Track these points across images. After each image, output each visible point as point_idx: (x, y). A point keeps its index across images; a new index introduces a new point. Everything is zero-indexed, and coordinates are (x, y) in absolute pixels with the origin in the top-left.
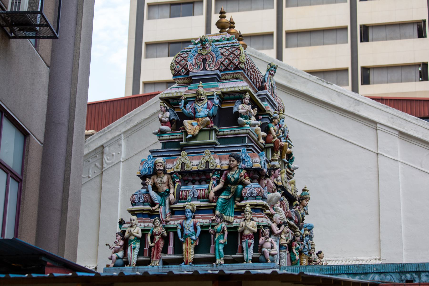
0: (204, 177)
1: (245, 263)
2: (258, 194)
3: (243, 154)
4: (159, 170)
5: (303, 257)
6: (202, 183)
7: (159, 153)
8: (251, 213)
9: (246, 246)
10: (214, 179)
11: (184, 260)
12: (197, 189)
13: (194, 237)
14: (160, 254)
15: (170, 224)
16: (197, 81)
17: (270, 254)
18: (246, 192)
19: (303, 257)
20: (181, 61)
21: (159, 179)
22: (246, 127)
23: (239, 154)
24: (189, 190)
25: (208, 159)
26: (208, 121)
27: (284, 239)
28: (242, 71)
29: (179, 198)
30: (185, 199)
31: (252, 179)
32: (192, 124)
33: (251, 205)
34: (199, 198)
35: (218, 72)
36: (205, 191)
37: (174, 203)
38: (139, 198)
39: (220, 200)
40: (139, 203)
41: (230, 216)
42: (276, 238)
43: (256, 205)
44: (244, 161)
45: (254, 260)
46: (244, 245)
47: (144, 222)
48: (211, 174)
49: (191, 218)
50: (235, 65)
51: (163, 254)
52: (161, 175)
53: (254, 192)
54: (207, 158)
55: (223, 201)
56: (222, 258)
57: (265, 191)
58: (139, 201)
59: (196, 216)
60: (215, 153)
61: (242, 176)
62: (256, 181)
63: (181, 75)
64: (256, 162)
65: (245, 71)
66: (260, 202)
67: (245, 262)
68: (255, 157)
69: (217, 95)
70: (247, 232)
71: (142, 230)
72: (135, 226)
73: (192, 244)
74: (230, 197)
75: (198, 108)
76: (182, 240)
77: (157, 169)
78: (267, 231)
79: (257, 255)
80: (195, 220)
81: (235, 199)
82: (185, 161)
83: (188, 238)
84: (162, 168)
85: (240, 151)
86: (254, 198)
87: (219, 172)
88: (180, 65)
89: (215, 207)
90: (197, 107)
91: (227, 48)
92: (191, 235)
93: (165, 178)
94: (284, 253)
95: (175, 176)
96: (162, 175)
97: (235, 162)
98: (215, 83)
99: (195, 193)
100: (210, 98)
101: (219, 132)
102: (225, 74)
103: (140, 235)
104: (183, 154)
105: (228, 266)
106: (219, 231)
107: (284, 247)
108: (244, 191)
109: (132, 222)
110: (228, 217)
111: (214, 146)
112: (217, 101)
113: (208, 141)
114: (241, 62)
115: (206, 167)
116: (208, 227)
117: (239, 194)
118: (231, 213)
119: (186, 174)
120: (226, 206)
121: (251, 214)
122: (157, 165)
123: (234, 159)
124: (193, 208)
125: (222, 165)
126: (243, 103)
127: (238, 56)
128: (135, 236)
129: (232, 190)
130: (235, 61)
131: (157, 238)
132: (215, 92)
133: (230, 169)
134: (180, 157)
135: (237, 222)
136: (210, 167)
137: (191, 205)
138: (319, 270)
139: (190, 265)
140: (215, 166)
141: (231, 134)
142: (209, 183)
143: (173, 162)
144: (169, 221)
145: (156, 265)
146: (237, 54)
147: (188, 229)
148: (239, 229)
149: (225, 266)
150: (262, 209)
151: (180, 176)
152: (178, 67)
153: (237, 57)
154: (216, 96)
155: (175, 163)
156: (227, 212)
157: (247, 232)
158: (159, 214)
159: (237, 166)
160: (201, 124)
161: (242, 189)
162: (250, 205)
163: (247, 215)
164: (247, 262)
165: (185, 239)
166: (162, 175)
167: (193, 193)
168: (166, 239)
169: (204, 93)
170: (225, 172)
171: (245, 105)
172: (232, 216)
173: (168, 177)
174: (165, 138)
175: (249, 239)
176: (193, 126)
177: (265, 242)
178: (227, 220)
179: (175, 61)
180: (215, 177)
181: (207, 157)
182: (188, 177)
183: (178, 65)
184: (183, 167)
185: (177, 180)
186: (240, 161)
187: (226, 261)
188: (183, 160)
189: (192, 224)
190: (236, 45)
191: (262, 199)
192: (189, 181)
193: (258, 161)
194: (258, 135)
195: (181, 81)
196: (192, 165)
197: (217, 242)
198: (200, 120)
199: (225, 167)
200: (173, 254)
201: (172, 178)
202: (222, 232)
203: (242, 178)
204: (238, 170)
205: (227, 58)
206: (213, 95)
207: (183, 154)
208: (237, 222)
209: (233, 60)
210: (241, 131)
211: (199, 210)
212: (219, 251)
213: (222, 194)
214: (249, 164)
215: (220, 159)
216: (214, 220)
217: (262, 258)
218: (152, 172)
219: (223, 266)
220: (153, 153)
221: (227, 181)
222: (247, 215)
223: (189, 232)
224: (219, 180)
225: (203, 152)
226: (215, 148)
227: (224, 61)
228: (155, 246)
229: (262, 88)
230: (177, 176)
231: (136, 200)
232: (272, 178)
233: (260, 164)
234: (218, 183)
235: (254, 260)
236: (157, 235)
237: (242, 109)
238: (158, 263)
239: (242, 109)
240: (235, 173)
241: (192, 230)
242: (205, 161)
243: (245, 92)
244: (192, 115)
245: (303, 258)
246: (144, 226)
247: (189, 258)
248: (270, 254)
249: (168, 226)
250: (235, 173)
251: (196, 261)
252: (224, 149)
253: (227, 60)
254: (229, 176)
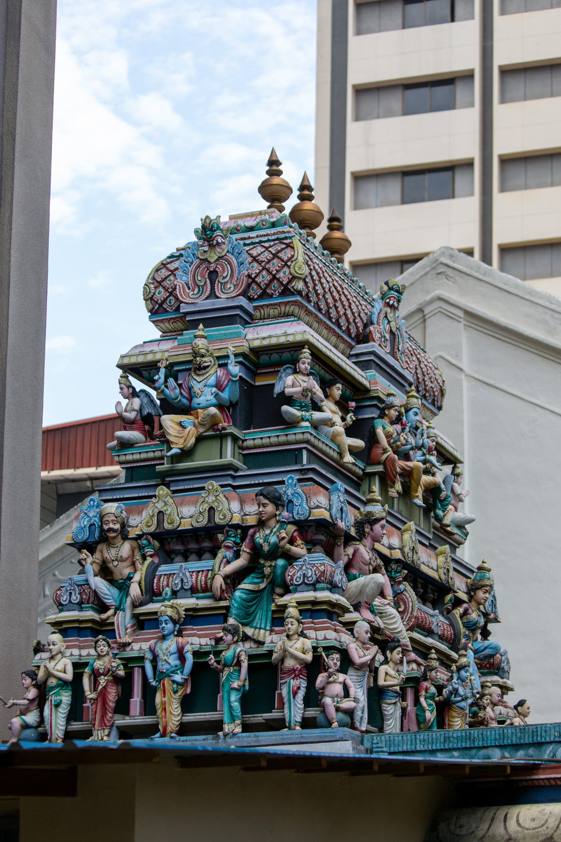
0: (207, 544)
1: (286, 729)
2: (320, 577)
3: (291, 488)
4: (110, 530)
5: (454, 714)
6: (204, 557)
7: (117, 492)
9: (289, 692)
10: (228, 547)
11: (160, 727)
12: (188, 571)
13: (178, 678)
14: (110, 715)
15: (132, 649)
16: (194, 325)
17: (338, 709)
18: (294, 574)
19: (454, 714)
20: (166, 278)
21: (113, 552)
22: (301, 427)
23: (281, 489)
24: (174, 574)
25: (213, 502)
26: (213, 416)
27: (391, 676)
28: (298, 298)
29: (151, 593)
30: (160, 594)
31: (311, 545)
32: (180, 424)
33: (299, 603)
34: (194, 591)
35: (243, 301)
36: (207, 575)
37: (141, 604)
38: (71, 593)
39: (238, 594)
40: (70, 606)
41: (260, 628)
42: (360, 673)
43: (314, 603)
44: (291, 504)
45: (307, 723)
46: (284, 691)
47: (80, 648)
48: (220, 537)
49: (172, 636)
50: (281, 283)
51: (117, 716)
52: (116, 541)
53: (309, 575)
54: (210, 501)
55: (244, 596)
56: (238, 722)
57: (338, 571)
58: (70, 602)
59: (185, 630)
60: (235, 488)
61: (283, 538)
62: (318, 548)
63: (166, 311)
64: (318, 507)
66: (324, 595)
67: (286, 727)
68: (315, 494)
69: (236, 355)
70: (290, 663)
71: (75, 665)
72: (60, 655)
73: (175, 692)
74: (262, 586)
75: (197, 388)
76: (154, 683)
77: (106, 527)
78: (333, 661)
79: (312, 712)
80: (180, 639)
81: (273, 592)
82: (165, 508)
83: (166, 679)
84: (117, 526)
85: (282, 482)
86: (311, 587)
87: (239, 531)
88: (164, 288)
89: (228, 608)
90: (193, 383)
91: (267, 245)
92: (173, 672)
93: (126, 549)
94: (391, 706)
95: (145, 542)
96: (119, 541)
97: (270, 508)
98: (238, 328)
99: (185, 581)
100: (222, 362)
101: (243, 441)
102: (262, 306)
103: (69, 676)
104: (161, 492)
105: (250, 737)
106: (229, 663)
107: (391, 694)
108: (291, 572)
109: (51, 647)
110: (257, 630)
111: (231, 472)
112: (235, 369)
113: (217, 461)
114: (294, 278)
115: (209, 521)
116: (207, 653)
117: (279, 580)
118: (263, 622)
119: (172, 538)
120: (254, 607)
121: (299, 622)
122: (105, 519)
123: (267, 501)
124: (178, 613)
125: (245, 515)
126: (297, 373)
127: (289, 263)
128: (59, 679)
129: (267, 571)
130: (281, 275)
131: (103, 681)
132: (231, 348)
133: (261, 524)
134: (154, 500)
135: (273, 641)
136: (217, 520)
137: (172, 607)
138: (442, 740)
139: (172, 737)
140: (228, 518)
142: (214, 556)
143: (140, 513)
144: (129, 644)
145: (102, 739)
146: (285, 259)
147: (165, 660)
148: (275, 656)
149: (243, 737)
150: (332, 611)
151: (157, 544)
152: (159, 293)
153: (286, 264)
154: (232, 357)
155: (144, 513)
156: (256, 621)
157: (290, 663)
158: (114, 630)
159: (276, 515)
160: (201, 424)
161: (285, 569)
162: (297, 602)
163: (290, 626)
164: (289, 728)
165: (160, 680)
166: (119, 541)
167: (182, 580)
168: (124, 684)
169: (208, 351)
170: (251, 531)
171: (300, 377)
172: (265, 629)
173: (131, 545)
174: (129, 458)
175: (293, 678)
176: (184, 428)
177: (329, 683)
178: (255, 637)
179: (154, 278)
180: (229, 543)
181: (211, 498)
182: (172, 543)
183: (161, 289)
184: (160, 522)
185: (149, 551)
186: (283, 506)
187: (247, 728)
188: (160, 505)
189: (173, 648)
190: (286, 238)
191: (330, 591)
192: (177, 553)
193: (325, 503)
195: (167, 325)
196: (182, 518)
197: (227, 686)
198: (199, 414)
199: (252, 521)
200: (141, 715)
201: (141, 548)
202: (235, 665)
203: (282, 543)
204: (278, 526)
205: (264, 268)
206: (227, 357)
207: (161, 492)
208: (272, 642)
209: (278, 271)
210: (291, 438)
211: (193, 617)
212: (230, 707)
213: (245, 581)
214: (301, 510)
215: (242, 502)
216: (221, 639)
217: (321, 719)
218: (97, 535)
219: (239, 737)
220: (103, 494)
221: (256, 552)
222: (290, 626)
223: (167, 666)
224: (239, 550)
225: (203, 488)
226: (234, 478)
227: (257, 275)
228: (97, 698)
230: (150, 542)
231: (64, 599)
233: (329, 510)
234: (237, 555)
235: (307, 723)
236: (102, 674)
237: (293, 386)
238: (108, 735)
239: (293, 386)
240: (271, 531)
241: (174, 661)
242: (206, 506)
243: (299, 346)
244: (184, 405)
245: (454, 717)
246: (80, 656)
247: (170, 724)
248: (338, 709)
249: (129, 653)
250: (271, 531)
251: (185, 729)
252: (254, 478)
253: (264, 273)
254: (258, 540)
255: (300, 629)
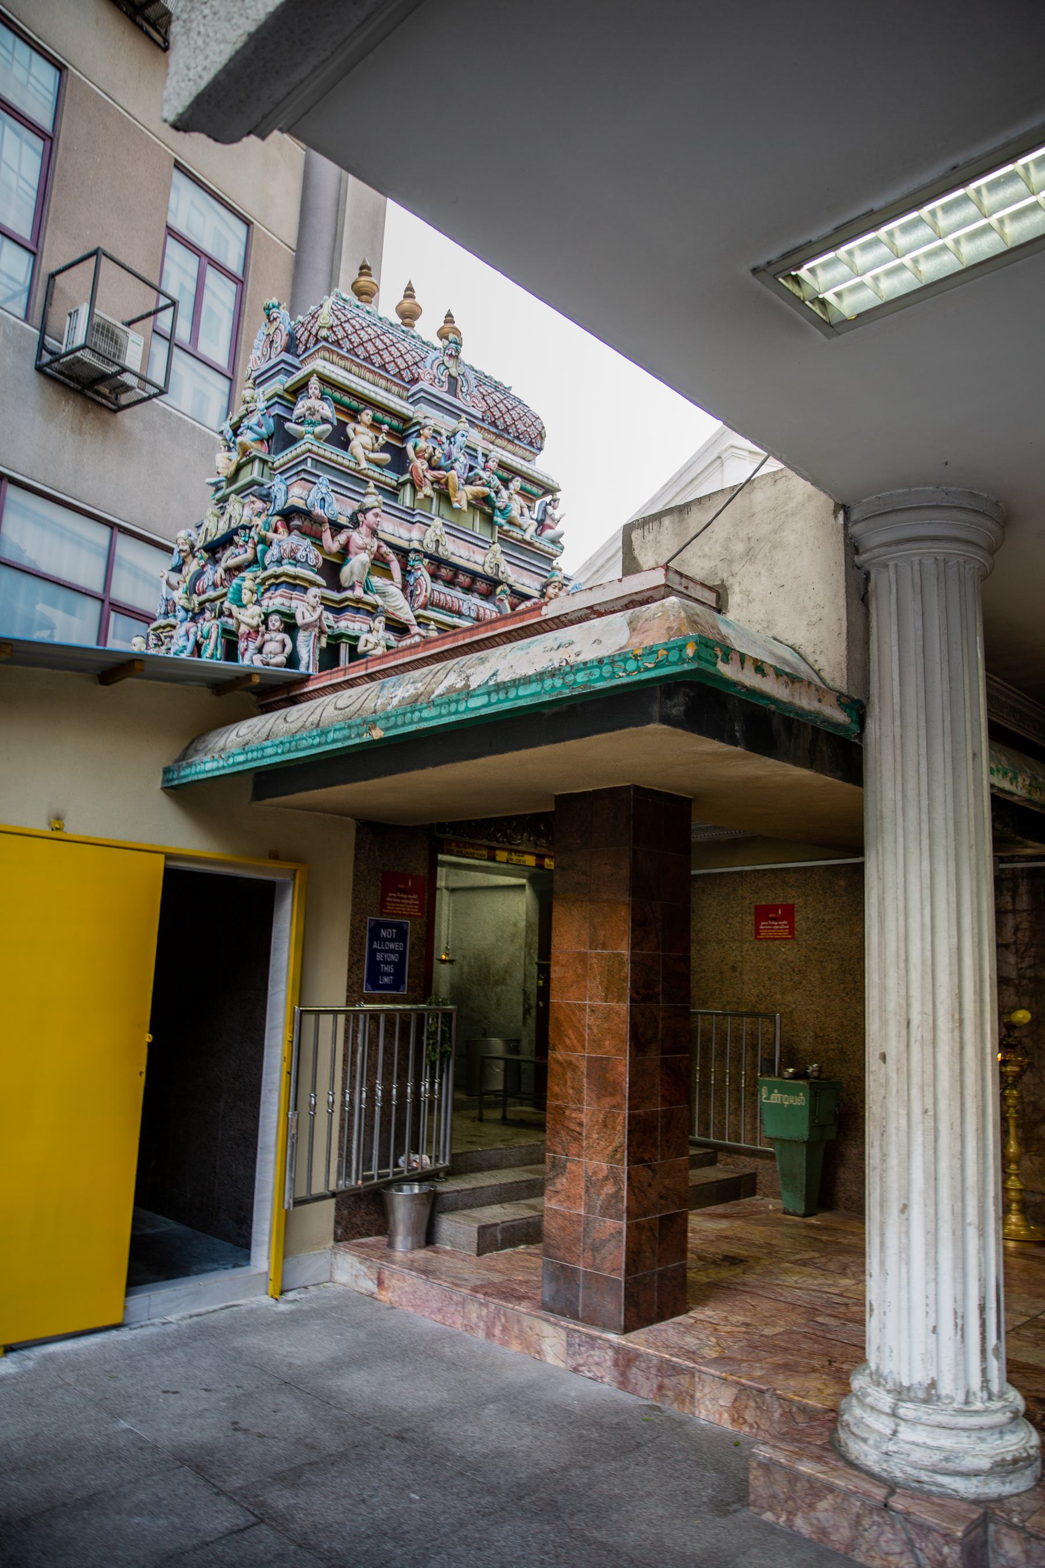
8: (250, 590)
42: (306, 633)
65: (337, 343)
70: (243, 629)
78: (275, 621)
84: (187, 547)
141: (289, 462)
194: (355, 458)
210: (299, 451)
229: (414, 381)
232: (363, 529)
255: (255, 599)
